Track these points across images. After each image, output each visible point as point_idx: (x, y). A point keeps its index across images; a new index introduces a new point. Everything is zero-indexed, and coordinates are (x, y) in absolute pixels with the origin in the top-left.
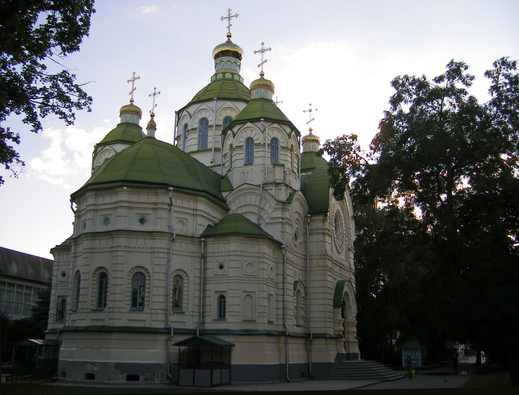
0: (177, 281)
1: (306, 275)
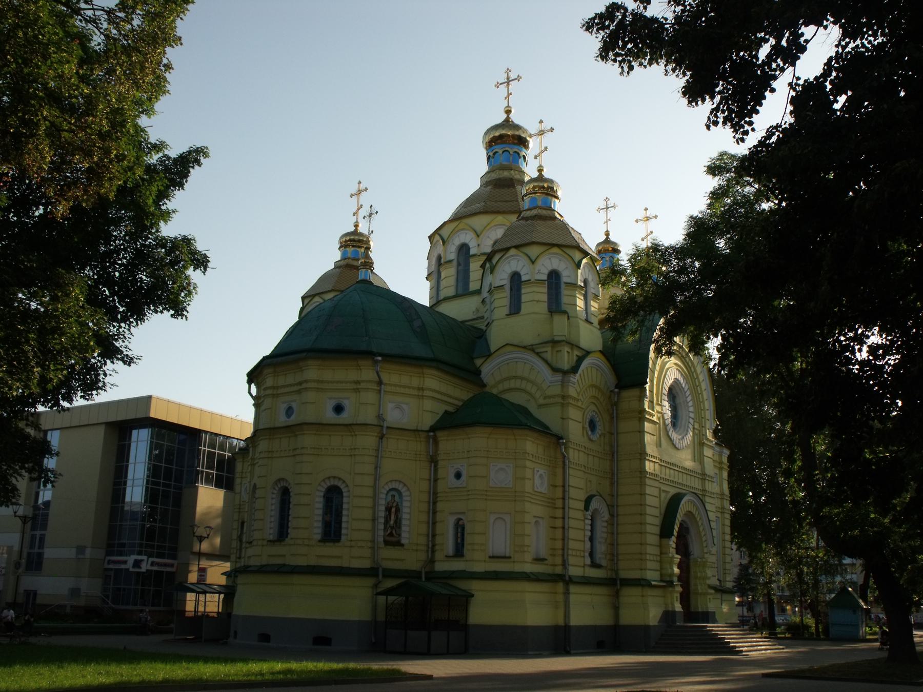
0: (393, 496)
1: (612, 484)
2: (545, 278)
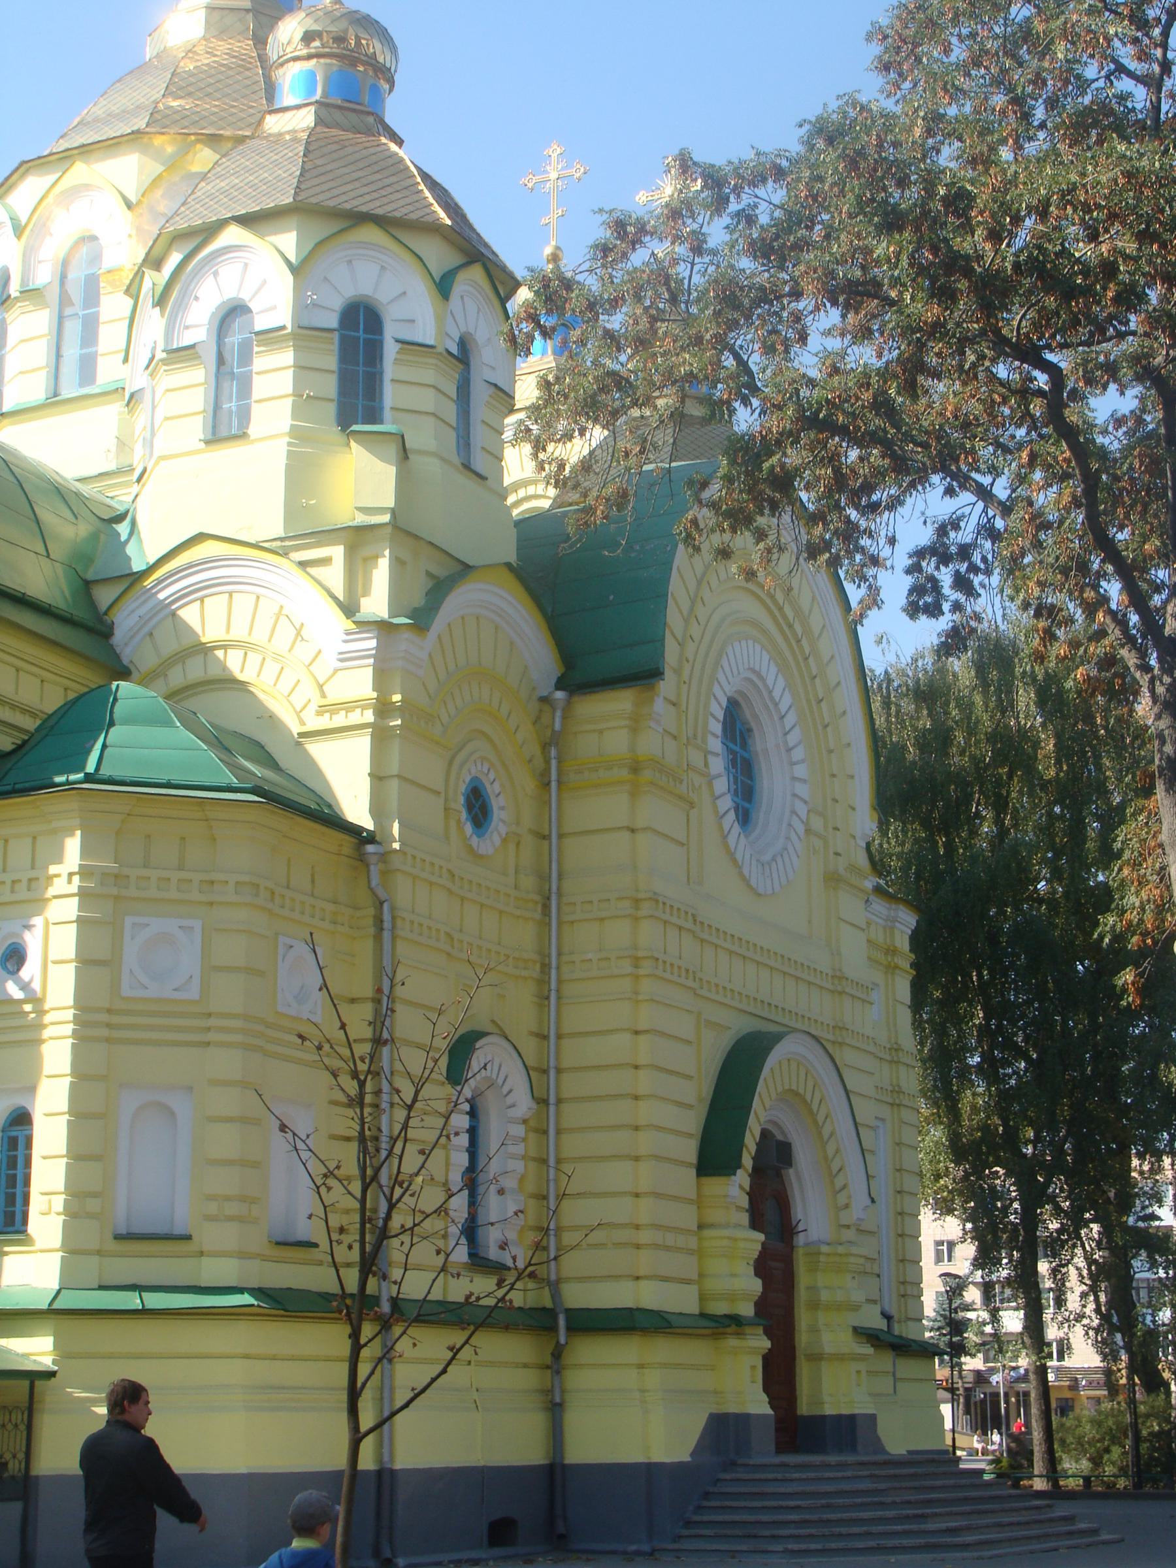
2: (333, 321)
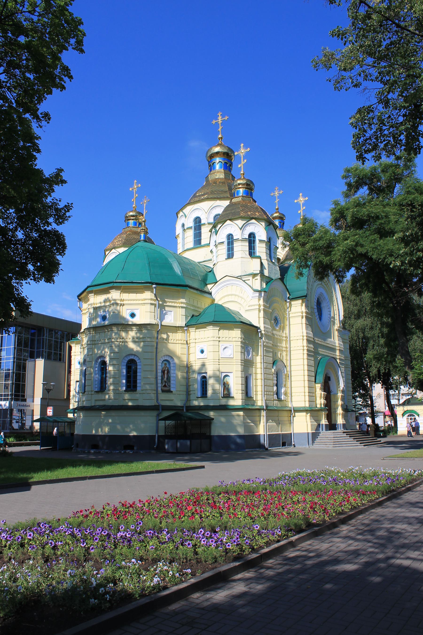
0: (166, 364)
